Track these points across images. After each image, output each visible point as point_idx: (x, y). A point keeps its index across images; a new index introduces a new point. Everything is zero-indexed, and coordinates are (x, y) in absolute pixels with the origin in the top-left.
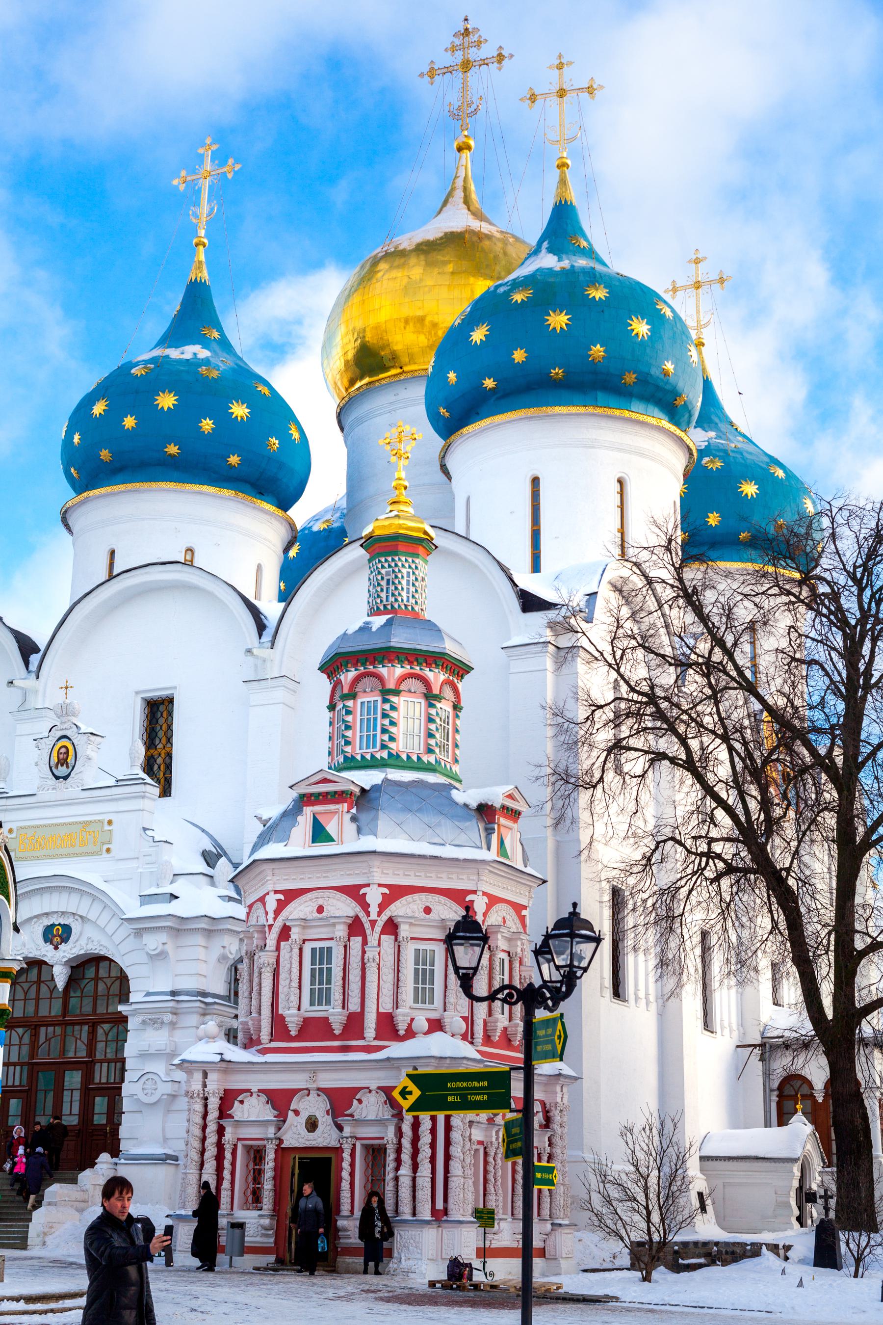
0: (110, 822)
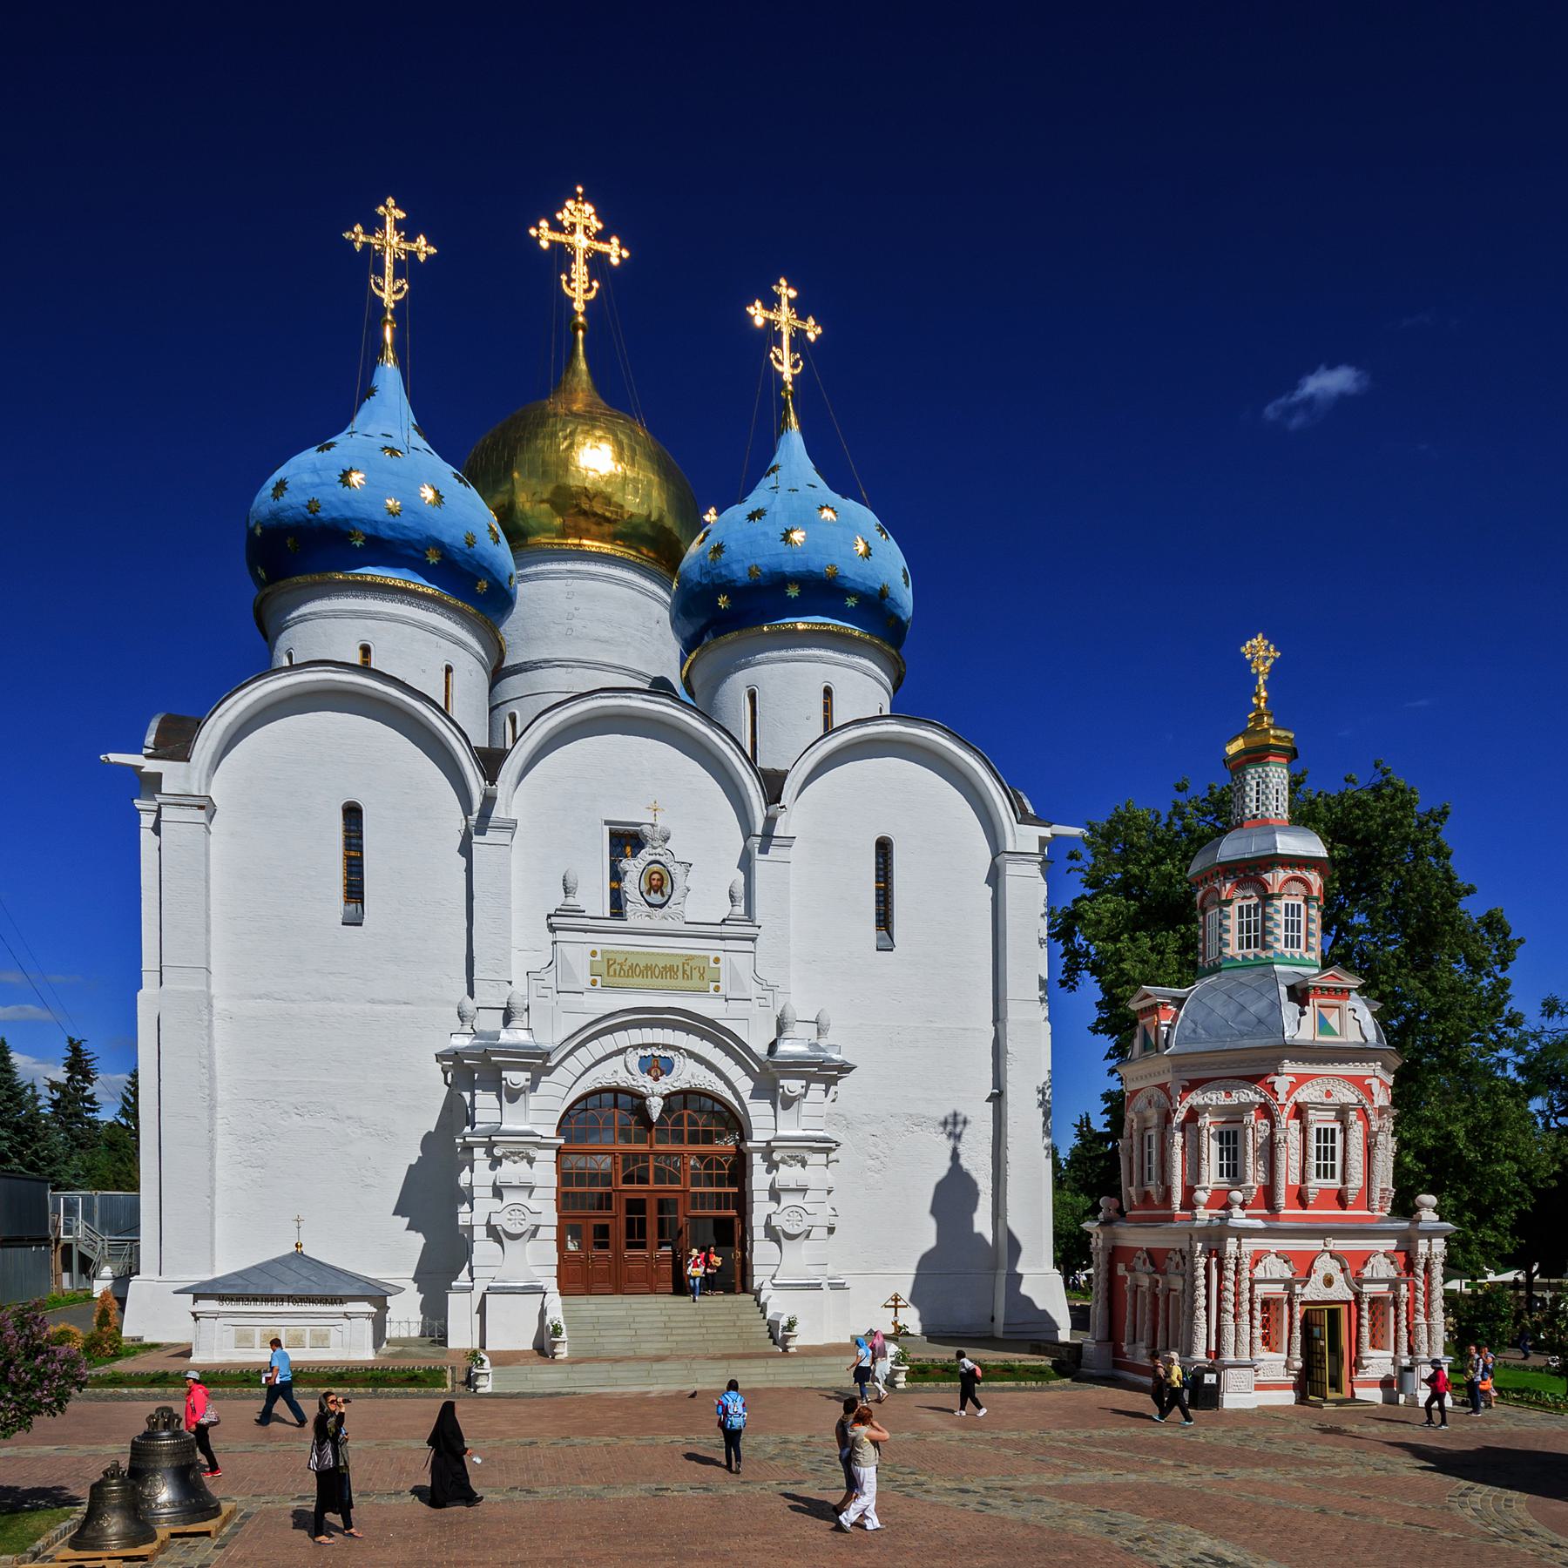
0: (717, 960)
